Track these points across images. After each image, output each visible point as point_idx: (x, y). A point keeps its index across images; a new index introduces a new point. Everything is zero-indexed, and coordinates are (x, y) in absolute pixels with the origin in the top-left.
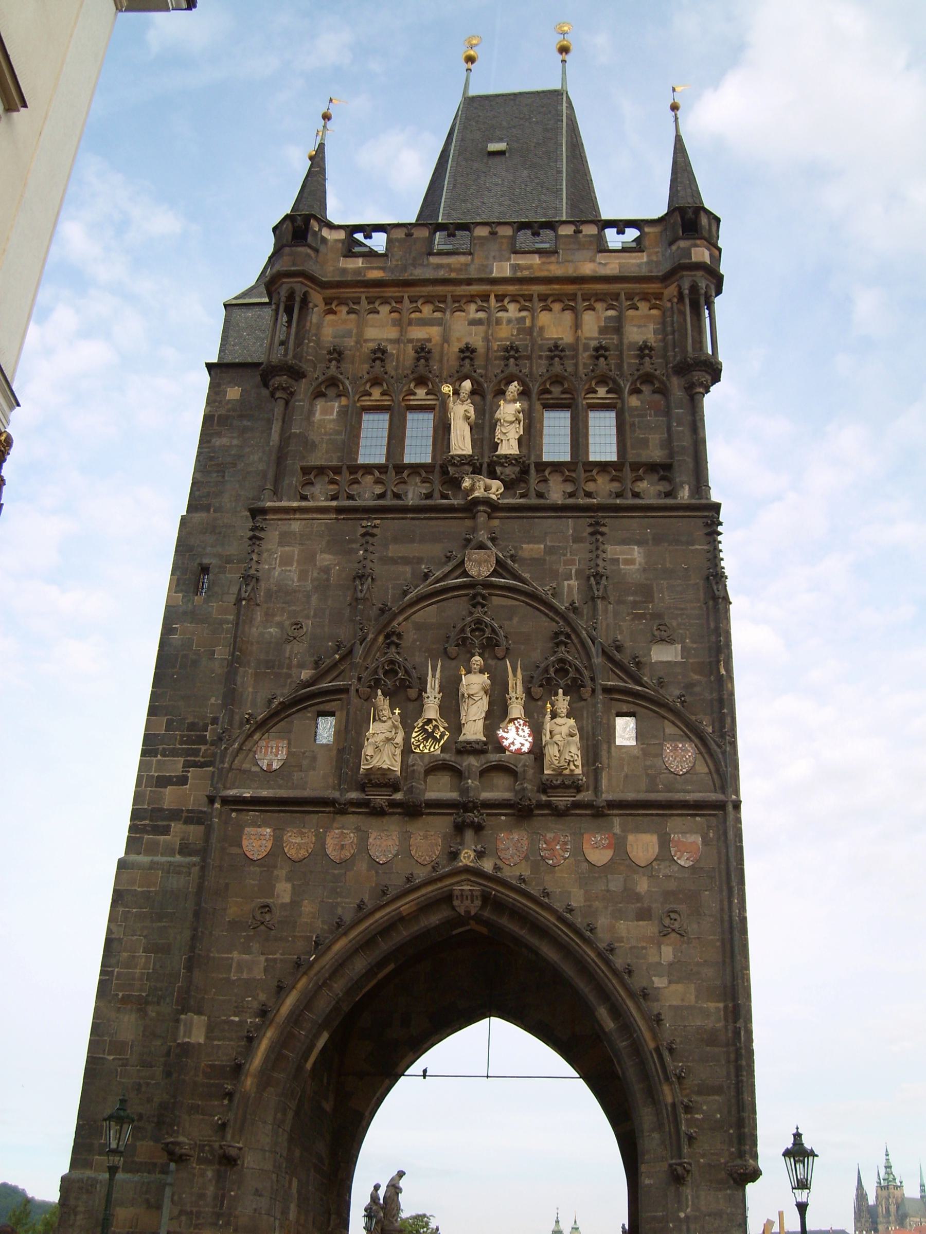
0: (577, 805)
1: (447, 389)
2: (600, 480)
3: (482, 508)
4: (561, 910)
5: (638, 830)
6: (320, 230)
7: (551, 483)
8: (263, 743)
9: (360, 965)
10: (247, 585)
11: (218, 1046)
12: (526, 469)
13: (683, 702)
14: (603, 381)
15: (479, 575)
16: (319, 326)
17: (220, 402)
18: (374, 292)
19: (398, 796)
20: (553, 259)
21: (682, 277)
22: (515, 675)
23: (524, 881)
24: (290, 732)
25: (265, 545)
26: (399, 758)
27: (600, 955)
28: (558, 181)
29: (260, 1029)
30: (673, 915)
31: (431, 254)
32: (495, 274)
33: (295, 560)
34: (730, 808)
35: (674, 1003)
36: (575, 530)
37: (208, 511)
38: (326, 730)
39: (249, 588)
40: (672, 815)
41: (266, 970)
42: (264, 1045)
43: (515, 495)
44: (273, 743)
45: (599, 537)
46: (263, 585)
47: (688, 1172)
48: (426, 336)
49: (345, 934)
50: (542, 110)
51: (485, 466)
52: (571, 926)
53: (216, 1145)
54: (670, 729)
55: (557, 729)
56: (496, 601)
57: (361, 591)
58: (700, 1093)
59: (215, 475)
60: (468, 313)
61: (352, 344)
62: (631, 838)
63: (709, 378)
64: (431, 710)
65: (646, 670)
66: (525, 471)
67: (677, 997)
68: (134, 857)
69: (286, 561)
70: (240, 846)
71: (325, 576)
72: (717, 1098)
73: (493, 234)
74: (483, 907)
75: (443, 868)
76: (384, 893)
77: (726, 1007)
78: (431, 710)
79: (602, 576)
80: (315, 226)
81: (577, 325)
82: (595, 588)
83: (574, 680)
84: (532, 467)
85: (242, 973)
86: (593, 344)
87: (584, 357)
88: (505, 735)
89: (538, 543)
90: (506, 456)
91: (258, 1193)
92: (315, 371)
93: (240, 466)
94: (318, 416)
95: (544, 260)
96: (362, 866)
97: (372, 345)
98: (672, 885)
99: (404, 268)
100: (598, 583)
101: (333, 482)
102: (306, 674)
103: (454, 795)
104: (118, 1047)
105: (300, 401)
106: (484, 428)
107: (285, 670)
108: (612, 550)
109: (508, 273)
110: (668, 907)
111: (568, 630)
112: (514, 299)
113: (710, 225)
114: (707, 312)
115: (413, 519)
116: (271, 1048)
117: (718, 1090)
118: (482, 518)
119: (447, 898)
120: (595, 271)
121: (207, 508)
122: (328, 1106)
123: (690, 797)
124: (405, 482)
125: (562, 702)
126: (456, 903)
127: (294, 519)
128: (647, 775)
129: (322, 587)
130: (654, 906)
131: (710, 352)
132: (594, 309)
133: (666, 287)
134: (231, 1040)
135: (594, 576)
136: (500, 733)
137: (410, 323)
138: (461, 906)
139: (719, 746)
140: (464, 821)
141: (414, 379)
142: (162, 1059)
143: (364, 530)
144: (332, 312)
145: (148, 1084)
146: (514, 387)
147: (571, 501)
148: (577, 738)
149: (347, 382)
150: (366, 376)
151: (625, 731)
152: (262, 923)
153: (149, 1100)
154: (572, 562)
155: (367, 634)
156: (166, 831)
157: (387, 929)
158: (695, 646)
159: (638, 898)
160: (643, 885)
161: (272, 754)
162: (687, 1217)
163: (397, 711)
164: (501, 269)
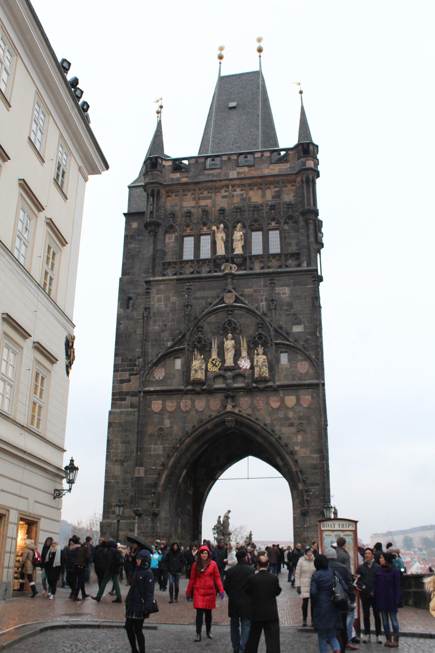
0: (266, 387)
1: (214, 228)
2: (273, 261)
3: (229, 276)
4: (262, 425)
5: (289, 395)
6: (162, 162)
7: (255, 263)
8: (156, 370)
9: (195, 447)
10: (146, 311)
11: (149, 477)
12: (246, 260)
13: (304, 348)
14: (273, 220)
15: (229, 302)
16: (165, 202)
17: (130, 229)
18: (184, 187)
19: (205, 387)
20: (253, 168)
21: (303, 174)
22: (243, 340)
23: (249, 415)
24: (165, 365)
25: (152, 295)
26: (204, 374)
27: (276, 440)
28: (257, 120)
29: (163, 470)
30: (301, 425)
31: (206, 169)
32: (231, 177)
33: (163, 301)
34: (321, 386)
35: (302, 455)
36: (264, 282)
37: (129, 275)
38: (178, 364)
39: (147, 313)
40: (300, 389)
41: (163, 450)
42: (164, 476)
43: (242, 269)
44: (160, 370)
45: (273, 285)
46: (152, 311)
47: (307, 512)
48: (206, 204)
49: (189, 437)
50: (251, 83)
51: (230, 258)
52: (266, 430)
53: (151, 510)
54: (300, 357)
55: (259, 360)
56: (236, 312)
57: (187, 311)
58: (311, 486)
59: (130, 260)
60: (221, 193)
61: (178, 209)
62: (286, 398)
63: (314, 216)
64: (214, 355)
65: (291, 335)
66: (245, 259)
67: (303, 453)
68: (114, 410)
69: (159, 300)
70: (151, 408)
71: (174, 306)
72: (317, 487)
73: (229, 159)
74: (236, 425)
75: (222, 412)
76: (202, 422)
77: (320, 456)
78: (214, 355)
79: (274, 301)
80: (160, 161)
81: (264, 196)
82: (271, 305)
83: (265, 341)
84: (248, 258)
85: (155, 451)
86: (270, 203)
87: (266, 209)
88: (241, 363)
89: (251, 288)
90: (237, 255)
91: (165, 525)
92: (164, 222)
93: (140, 256)
94: (167, 241)
95: (250, 169)
96: (193, 413)
97: (185, 209)
98: (302, 414)
99: (196, 177)
100: (273, 303)
101: (174, 268)
102: (169, 344)
103: (223, 386)
104: (115, 477)
105: (160, 235)
106: (229, 244)
107: (162, 343)
108: (278, 289)
109: (235, 176)
110: (300, 422)
111: (262, 322)
112: (239, 186)
113: (314, 149)
115: (204, 281)
116: (167, 476)
117: (317, 484)
118: (229, 280)
119: (224, 422)
120: (269, 173)
121: (129, 274)
122: (191, 492)
123: (307, 382)
124: (201, 266)
125: (260, 350)
126: (227, 423)
127: (161, 284)
128: (292, 375)
129: (173, 310)
130: (295, 422)
132: (270, 188)
133: (298, 177)
134: (152, 475)
135: (271, 301)
136: (239, 362)
137: (199, 199)
138: (228, 425)
139: (316, 363)
140: (227, 395)
141: (202, 223)
142: (130, 481)
143: (187, 287)
144: (169, 196)
145: (126, 490)
147: (262, 271)
148: (266, 363)
149: (177, 227)
150: (184, 224)
151: (284, 358)
152: (161, 434)
153: (127, 495)
154: (263, 295)
155: (190, 328)
156: (124, 399)
157: (203, 434)
158: (308, 325)
159: (289, 419)
160: (291, 415)
161: (159, 374)
162: (307, 527)
163: (202, 357)
164: (233, 174)
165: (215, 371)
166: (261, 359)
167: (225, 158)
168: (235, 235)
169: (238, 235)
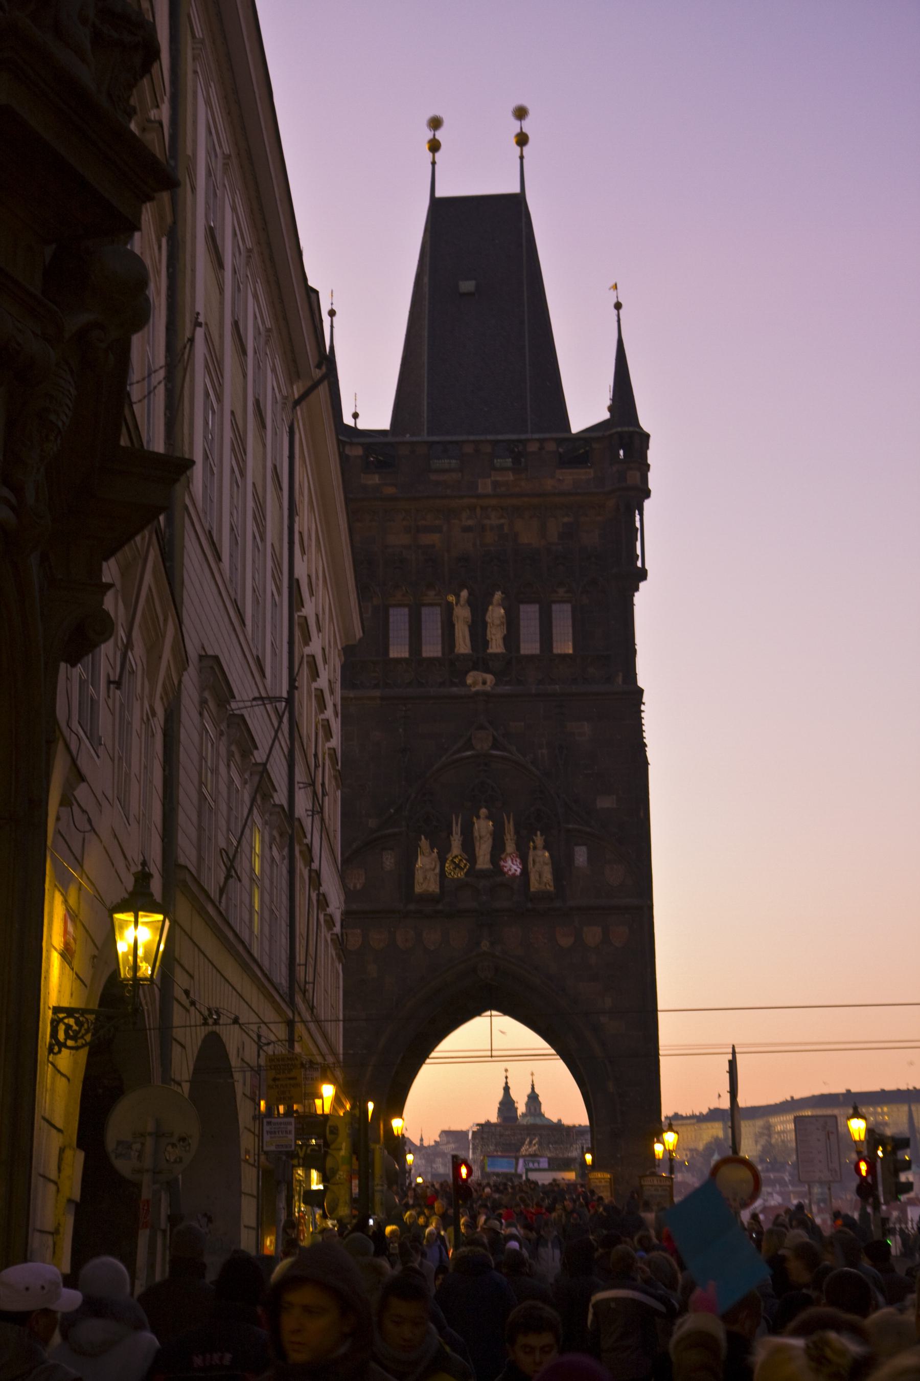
1: (451, 598)
12: (510, 664)
22: (509, 822)
32: (480, 491)
38: (389, 861)
64: (456, 849)
78: (456, 849)
90: (496, 655)
109: (489, 490)
114: (638, 518)
125: (539, 840)
131: (639, 564)
136: (502, 863)
146: (498, 596)
151: (581, 856)
163: (435, 850)
165: (458, 879)
166: (542, 857)
167: (468, 449)
168: (489, 614)
169: (496, 613)
